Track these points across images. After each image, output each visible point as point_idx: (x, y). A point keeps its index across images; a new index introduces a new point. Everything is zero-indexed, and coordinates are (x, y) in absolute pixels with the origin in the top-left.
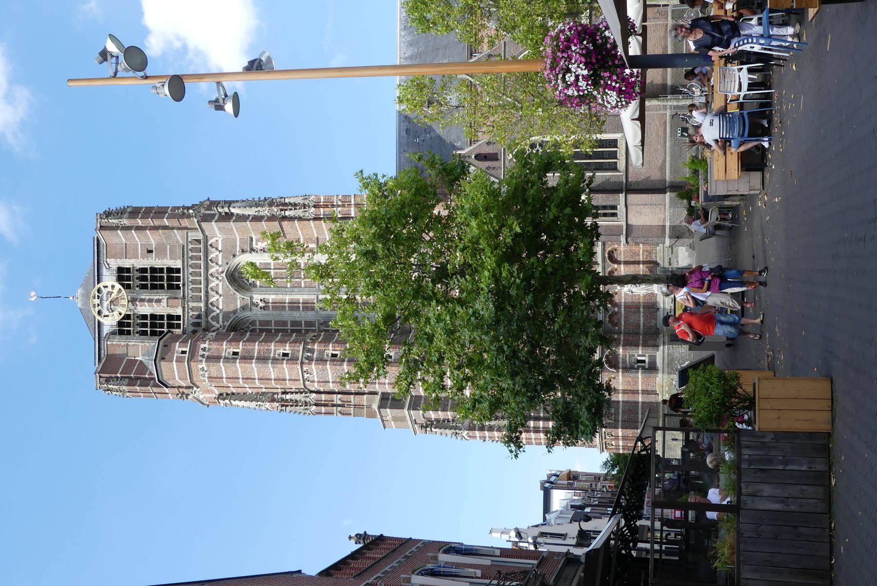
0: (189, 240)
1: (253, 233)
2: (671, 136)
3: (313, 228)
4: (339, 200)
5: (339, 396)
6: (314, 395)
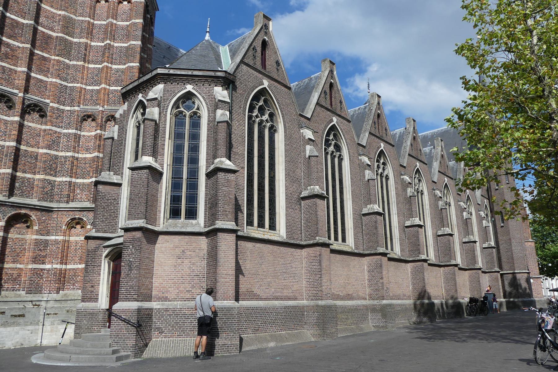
2: (286, 307)
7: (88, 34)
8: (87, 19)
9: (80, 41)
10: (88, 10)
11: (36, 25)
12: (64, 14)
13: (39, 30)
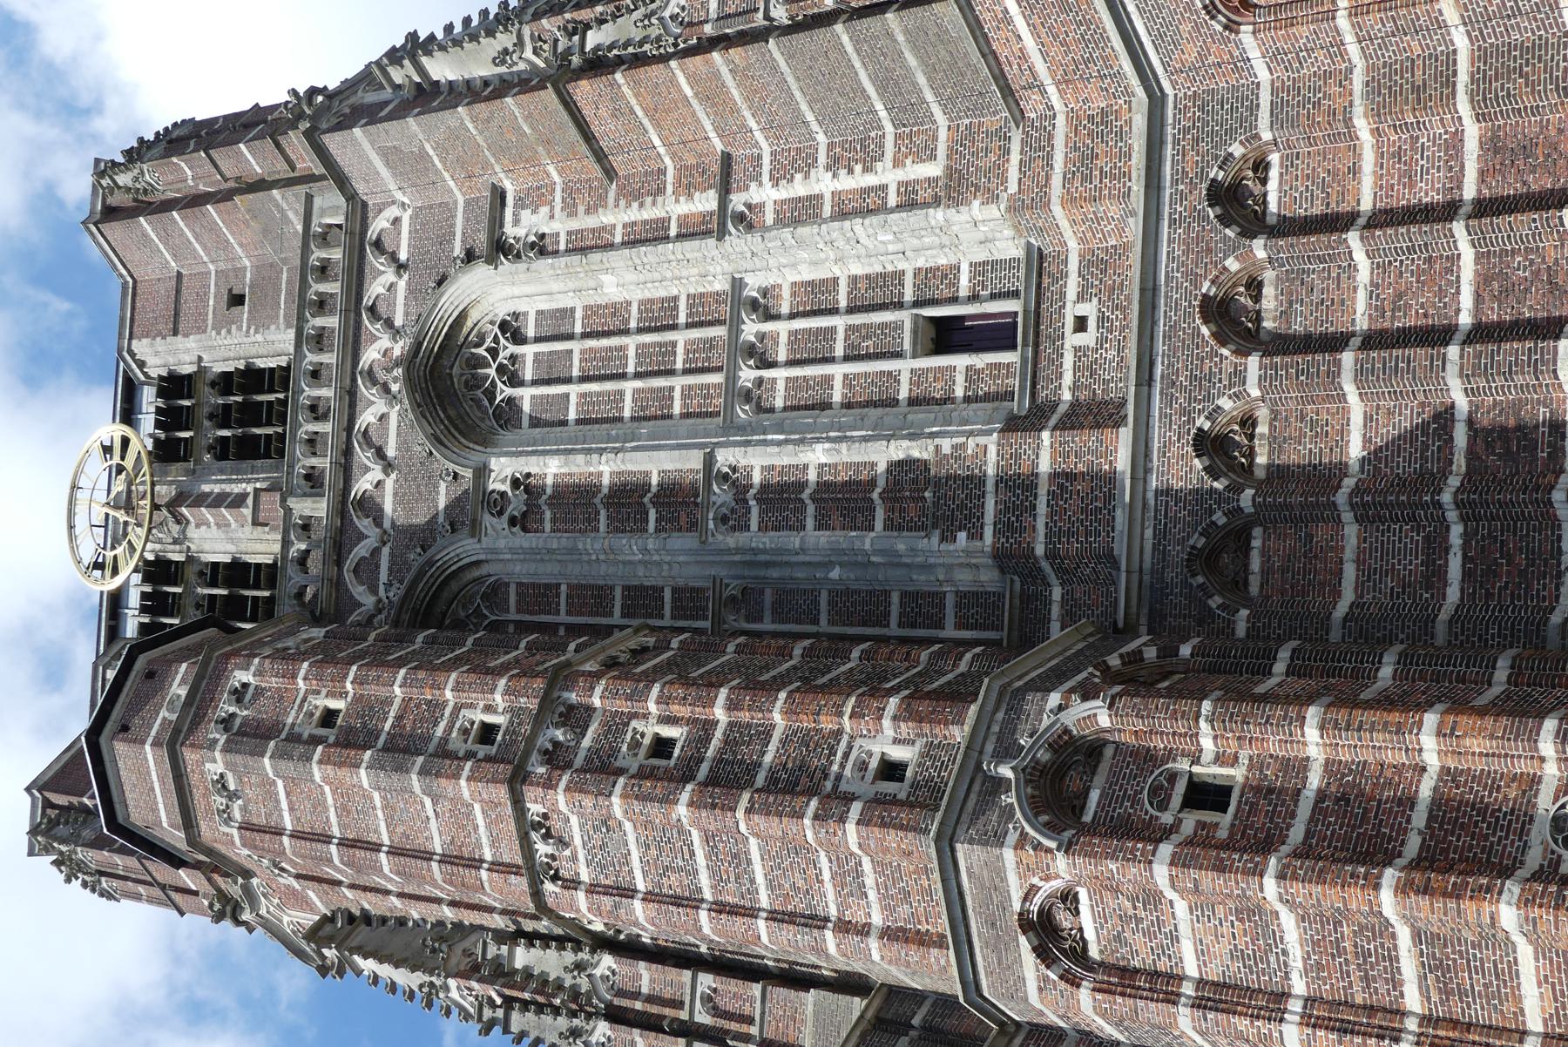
0: (316, 229)
1: (498, 169)
3: (695, 103)
5: (706, 980)
6: (607, 962)
8: (1342, 21)
9: (1457, 21)
10: (1304, 31)
11: (1465, 210)
13: (1479, 191)
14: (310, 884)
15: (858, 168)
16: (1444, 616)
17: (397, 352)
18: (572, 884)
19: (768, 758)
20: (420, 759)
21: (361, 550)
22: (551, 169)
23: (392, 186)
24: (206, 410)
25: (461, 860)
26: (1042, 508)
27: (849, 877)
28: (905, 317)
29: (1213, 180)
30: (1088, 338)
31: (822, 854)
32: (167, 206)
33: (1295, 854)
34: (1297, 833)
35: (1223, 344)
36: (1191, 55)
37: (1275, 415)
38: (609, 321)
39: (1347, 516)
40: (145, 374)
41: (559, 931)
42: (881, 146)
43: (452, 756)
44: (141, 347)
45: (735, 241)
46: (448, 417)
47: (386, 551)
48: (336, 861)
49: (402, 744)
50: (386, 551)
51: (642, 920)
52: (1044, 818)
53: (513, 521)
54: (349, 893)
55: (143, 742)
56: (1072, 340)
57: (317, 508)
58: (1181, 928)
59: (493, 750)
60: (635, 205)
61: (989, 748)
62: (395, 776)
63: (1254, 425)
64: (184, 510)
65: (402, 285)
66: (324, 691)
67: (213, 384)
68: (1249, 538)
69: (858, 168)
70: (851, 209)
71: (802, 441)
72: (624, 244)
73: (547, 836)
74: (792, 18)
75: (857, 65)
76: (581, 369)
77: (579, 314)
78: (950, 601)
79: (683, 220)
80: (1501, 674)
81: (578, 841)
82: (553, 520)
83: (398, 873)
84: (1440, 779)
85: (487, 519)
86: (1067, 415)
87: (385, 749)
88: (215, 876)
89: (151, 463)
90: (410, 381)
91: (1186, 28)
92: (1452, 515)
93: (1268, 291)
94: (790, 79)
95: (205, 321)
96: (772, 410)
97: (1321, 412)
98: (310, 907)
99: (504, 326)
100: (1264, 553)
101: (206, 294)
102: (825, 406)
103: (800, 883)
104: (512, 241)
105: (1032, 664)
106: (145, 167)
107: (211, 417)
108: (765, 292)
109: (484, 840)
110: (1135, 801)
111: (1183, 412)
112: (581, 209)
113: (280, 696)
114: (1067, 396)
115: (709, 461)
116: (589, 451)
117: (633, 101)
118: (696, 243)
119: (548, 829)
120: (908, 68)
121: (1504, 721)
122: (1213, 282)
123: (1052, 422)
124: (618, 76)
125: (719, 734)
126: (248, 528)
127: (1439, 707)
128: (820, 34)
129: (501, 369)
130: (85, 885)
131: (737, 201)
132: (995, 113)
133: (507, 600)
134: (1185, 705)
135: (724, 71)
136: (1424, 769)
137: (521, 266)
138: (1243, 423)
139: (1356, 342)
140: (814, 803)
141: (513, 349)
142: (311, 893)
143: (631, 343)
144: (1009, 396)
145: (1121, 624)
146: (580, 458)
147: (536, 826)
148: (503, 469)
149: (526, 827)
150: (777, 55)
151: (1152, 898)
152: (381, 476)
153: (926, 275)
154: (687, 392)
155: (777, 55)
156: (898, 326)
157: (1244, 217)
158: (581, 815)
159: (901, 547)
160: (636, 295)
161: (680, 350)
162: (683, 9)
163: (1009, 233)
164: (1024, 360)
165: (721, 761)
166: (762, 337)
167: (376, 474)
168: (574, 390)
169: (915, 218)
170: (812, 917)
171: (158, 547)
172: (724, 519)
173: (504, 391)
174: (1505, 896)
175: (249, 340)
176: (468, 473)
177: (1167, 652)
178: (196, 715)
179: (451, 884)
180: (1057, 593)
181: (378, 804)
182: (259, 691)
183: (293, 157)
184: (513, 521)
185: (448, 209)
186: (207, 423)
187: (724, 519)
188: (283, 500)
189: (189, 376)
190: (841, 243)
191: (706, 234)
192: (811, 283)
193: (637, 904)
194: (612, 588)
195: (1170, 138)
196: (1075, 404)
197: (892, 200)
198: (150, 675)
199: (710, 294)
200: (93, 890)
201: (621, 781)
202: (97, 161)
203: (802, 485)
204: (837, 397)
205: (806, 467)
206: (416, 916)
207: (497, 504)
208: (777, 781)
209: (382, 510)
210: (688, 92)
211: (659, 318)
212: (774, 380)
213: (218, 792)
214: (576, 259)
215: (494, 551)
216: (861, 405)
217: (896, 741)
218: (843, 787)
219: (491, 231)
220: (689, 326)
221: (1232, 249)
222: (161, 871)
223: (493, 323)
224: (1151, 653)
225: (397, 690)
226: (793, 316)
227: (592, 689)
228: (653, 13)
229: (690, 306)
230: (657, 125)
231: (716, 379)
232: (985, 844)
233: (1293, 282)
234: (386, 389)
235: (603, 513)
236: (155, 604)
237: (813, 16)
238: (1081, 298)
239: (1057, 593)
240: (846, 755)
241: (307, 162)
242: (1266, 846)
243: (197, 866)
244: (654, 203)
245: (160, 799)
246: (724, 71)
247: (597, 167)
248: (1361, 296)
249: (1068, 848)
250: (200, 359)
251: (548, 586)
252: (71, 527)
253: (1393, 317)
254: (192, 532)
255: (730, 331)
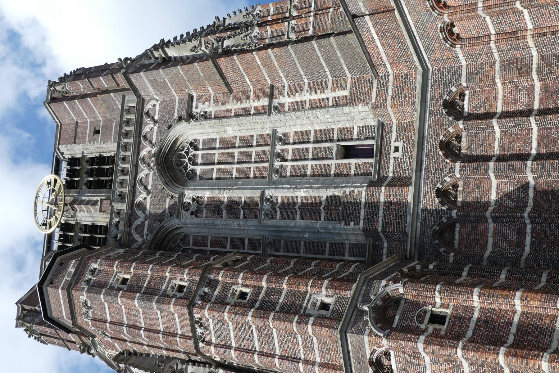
1: (191, 88)
3: (262, 67)
4: (295, 6)
7: (517, 38)
8: (492, 45)
9: (533, 46)
10: (479, 48)
12: (500, 78)
13: (540, 106)
14: (116, 340)
15: (319, 92)
16: (524, 257)
17: (153, 152)
18: (209, 343)
19: (281, 301)
20: (156, 297)
21: (138, 222)
22: (210, 89)
23: (153, 93)
24: (85, 171)
25: (170, 334)
26: (381, 214)
27: (308, 345)
28: (334, 145)
29: (445, 100)
30: (399, 155)
31: (299, 336)
32: (73, 98)
33: (469, 341)
34: (469, 333)
35: (447, 158)
36: (438, 55)
37: (465, 184)
38: (228, 144)
39: (490, 221)
40: (64, 157)
41: (204, 360)
42: (327, 84)
43: (168, 296)
44: (62, 148)
45: (274, 116)
46: (171, 176)
47: (147, 222)
48: (125, 332)
49: (150, 291)
50: (147, 222)
51: (234, 357)
52: (379, 325)
53: (192, 213)
54: (129, 344)
55: (58, 288)
56: (393, 155)
57: (123, 206)
58: (427, 366)
59: (183, 294)
60: (239, 102)
61: (360, 299)
62: (147, 303)
63: (457, 187)
64: (75, 206)
65: (156, 128)
66: (123, 272)
67: (87, 162)
68: (455, 227)
69: (319, 92)
70: (316, 106)
71: (296, 188)
72: (235, 116)
73: (201, 326)
74: (297, 38)
75: (320, 55)
76: (218, 160)
77: (218, 141)
78: (347, 247)
79: (256, 108)
80: (544, 279)
81: (212, 328)
82: (207, 213)
83: (147, 338)
84: (521, 315)
85: (183, 212)
86: (391, 181)
87: (144, 293)
88: (82, 337)
89: (64, 189)
90: (157, 162)
91: (437, 45)
92: (528, 221)
93: (464, 139)
94: (296, 60)
95: (85, 139)
96: (286, 177)
97: (483, 183)
98: (116, 349)
99: (191, 144)
100: (460, 232)
101: (86, 129)
102: (304, 176)
103: (291, 346)
104: (195, 114)
105: (376, 270)
106: (66, 84)
107: (86, 173)
108: (284, 135)
109: (178, 327)
110: (412, 320)
111: (432, 181)
112: (220, 103)
113: (108, 273)
114: (391, 175)
115: (263, 194)
116: (220, 189)
117: (240, 66)
118: (260, 117)
119: (201, 324)
120: (337, 57)
121: (545, 295)
122: (444, 136)
123: (385, 184)
124: (235, 57)
125: (263, 291)
126: (98, 213)
127: (522, 290)
128: (307, 44)
129: (190, 159)
130: (35, 338)
131: (275, 102)
132: (368, 73)
133: (189, 241)
134: (430, 286)
135: (272, 56)
136: (515, 312)
137: (198, 123)
138: (453, 186)
139: (494, 158)
140: (297, 317)
141: (194, 152)
142: (116, 344)
143: (236, 151)
144: (370, 174)
145: (408, 257)
146: (217, 192)
147: (197, 322)
148: (189, 195)
149: (193, 323)
150: (291, 51)
151: (417, 355)
152: (146, 196)
153: (342, 130)
154: (256, 169)
155: (291, 51)
156: (331, 148)
157: (456, 113)
158: (213, 319)
159: (330, 227)
160: (239, 134)
161: (253, 154)
162: (258, 34)
163: (371, 116)
164: (376, 161)
165: (264, 301)
166: (283, 150)
167: (144, 195)
168: (215, 167)
169: (339, 110)
170: (295, 358)
171: (66, 218)
172: (267, 215)
173: (191, 167)
174: (544, 359)
175: (101, 146)
176: (177, 196)
177: (425, 267)
178: (77, 279)
179: (166, 342)
180: (385, 245)
181: (141, 313)
182: (100, 271)
183: (119, 82)
184: (192, 213)
185: (173, 102)
186: (85, 175)
187: (267, 215)
188: (111, 203)
189: (79, 158)
190: (312, 118)
191: (264, 113)
192: (301, 132)
193: (232, 352)
194: (227, 238)
195: (430, 84)
196: (394, 178)
197: (331, 103)
198: (61, 264)
199: (265, 135)
200: (38, 340)
201: (228, 307)
202: (49, 81)
203: (295, 204)
204: (309, 173)
205: (297, 197)
206: (153, 353)
207: (187, 207)
208: (284, 309)
209: (146, 208)
210: (259, 63)
211: (247, 143)
212: (287, 166)
213: (84, 307)
214: (217, 121)
215: (185, 224)
216: (317, 176)
217: (327, 296)
218: (307, 312)
219: (188, 110)
220: (257, 146)
221: (451, 124)
222: (63, 334)
223: (187, 143)
224: (418, 267)
225: (149, 272)
226: (294, 143)
227: (218, 274)
228: (248, 35)
229: (257, 139)
230: (248, 75)
231: (266, 165)
232: (358, 334)
233: (473, 136)
234: (149, 165)
235: (224, 211)
236: (64, 239)
237: (304, 38)
238: (397, 140)
239: (385, 245)
240: (309, 301)
241: (124, 84)
242: (458, 337)
243: (76, 333)
244: (246, 102)
245: (63, 308)
246: (272, 56)
247: (226, 88)
248: (497, 142)
249: (387, 336)
250: (83, 152)
251: (204, 237)
252: (35, 211)
253: (508, 150)
254: (78, 214)
255: (271, 148)
